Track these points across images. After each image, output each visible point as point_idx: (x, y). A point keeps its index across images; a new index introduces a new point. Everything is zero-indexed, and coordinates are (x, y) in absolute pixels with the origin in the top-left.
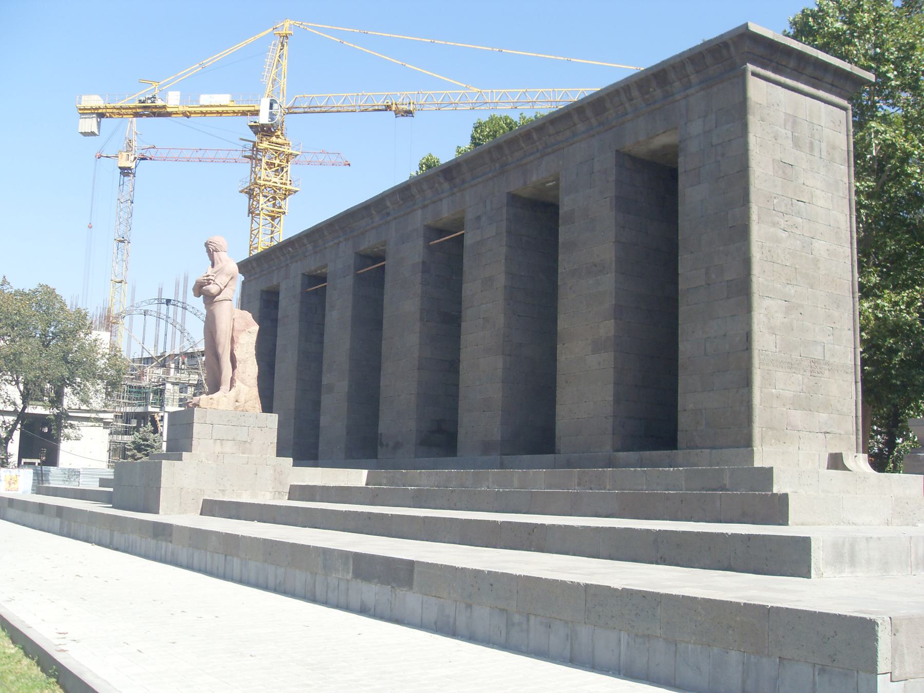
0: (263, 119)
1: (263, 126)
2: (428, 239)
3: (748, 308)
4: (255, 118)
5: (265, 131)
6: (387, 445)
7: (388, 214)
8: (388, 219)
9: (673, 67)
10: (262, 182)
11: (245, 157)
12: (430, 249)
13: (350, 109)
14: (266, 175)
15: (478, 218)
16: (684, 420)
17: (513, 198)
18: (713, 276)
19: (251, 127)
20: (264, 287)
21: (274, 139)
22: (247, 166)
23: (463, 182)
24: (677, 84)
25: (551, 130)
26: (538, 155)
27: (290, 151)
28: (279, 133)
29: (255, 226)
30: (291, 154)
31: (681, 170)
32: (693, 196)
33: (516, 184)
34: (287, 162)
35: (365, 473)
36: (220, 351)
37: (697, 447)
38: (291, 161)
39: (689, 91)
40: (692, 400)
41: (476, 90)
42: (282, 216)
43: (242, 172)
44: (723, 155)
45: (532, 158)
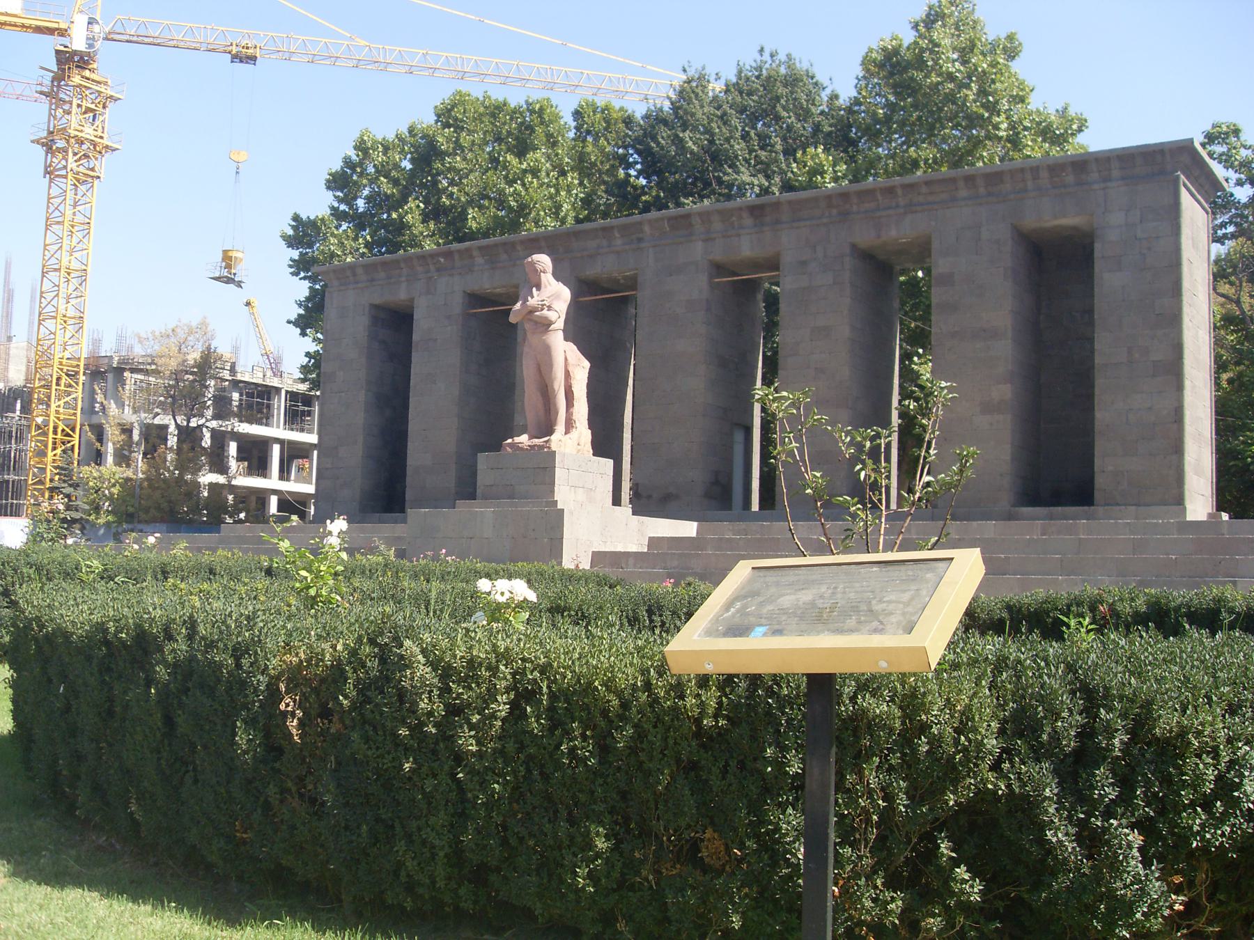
0: (78, 43)
1: (75, 53)
2: (711, 277)
3: (1180, 387)
4: (65, 41)
5: (69, 61)
6: (649, 497)
7: (640, 240)
8: (643, 245)
9: (1097, 160)
10: (73, 133)
11: (41, 93)
12: (713, 286)
13: (194, 45)
14: (74, 122)
15: (803, 263)
16: (1100, 481)
17: (854, 247)
18: (1137, 355)
19: (58, 52)
20: (377, 301)
21: (87, 73)
22: (44, 105)
23: (778, 222)
24: (1095, 176)
25: (924, 189)
26: (902, 210)
27: (110, 93)
28: (95, 66)
29: (55, 191)
30: (111, 97)
31: (1097, 254)
32: (1110, 281)
33: (865, 237)
34: (104, 107)
35: (695, 524)
36: (556, 387)
37: (1118, 504)
38: (110, 105)
39: (1109, 184)
40: (1109, 464)
41: (363, 43)
42: (96, 182)
43: (38, 115)
44: (1149, 249)
45: (891, 212)
